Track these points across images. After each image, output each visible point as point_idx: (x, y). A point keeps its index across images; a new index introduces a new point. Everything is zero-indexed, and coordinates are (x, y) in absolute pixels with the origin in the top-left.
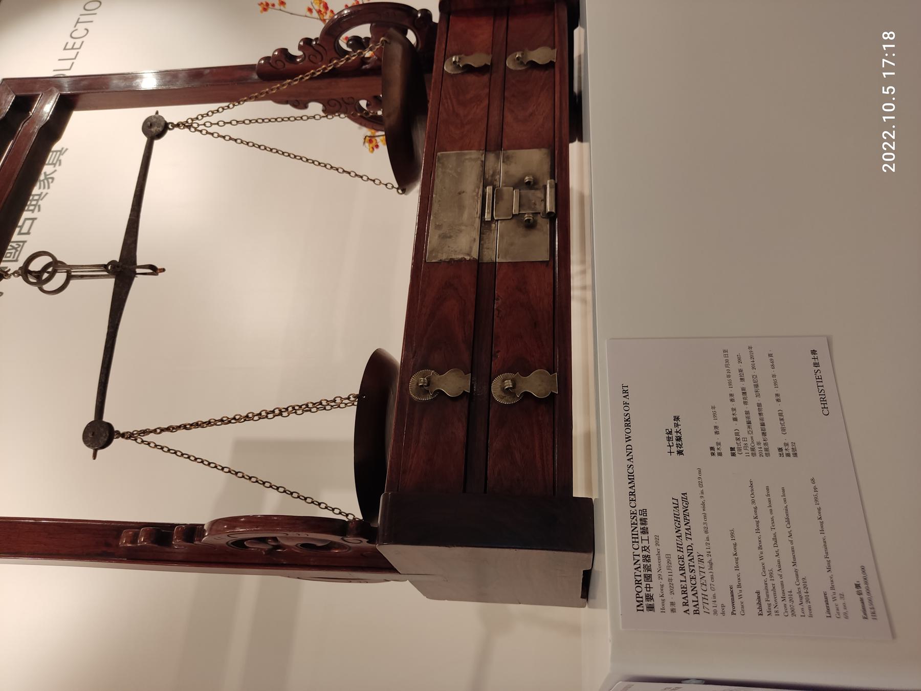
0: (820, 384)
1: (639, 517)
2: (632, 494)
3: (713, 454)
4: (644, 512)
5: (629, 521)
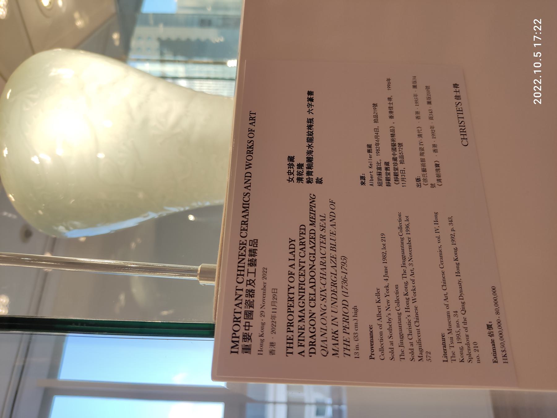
0: (460, 116)
1: (248, 247)
2: (245, 223)
4: (255, 242)
5: (237, 251)
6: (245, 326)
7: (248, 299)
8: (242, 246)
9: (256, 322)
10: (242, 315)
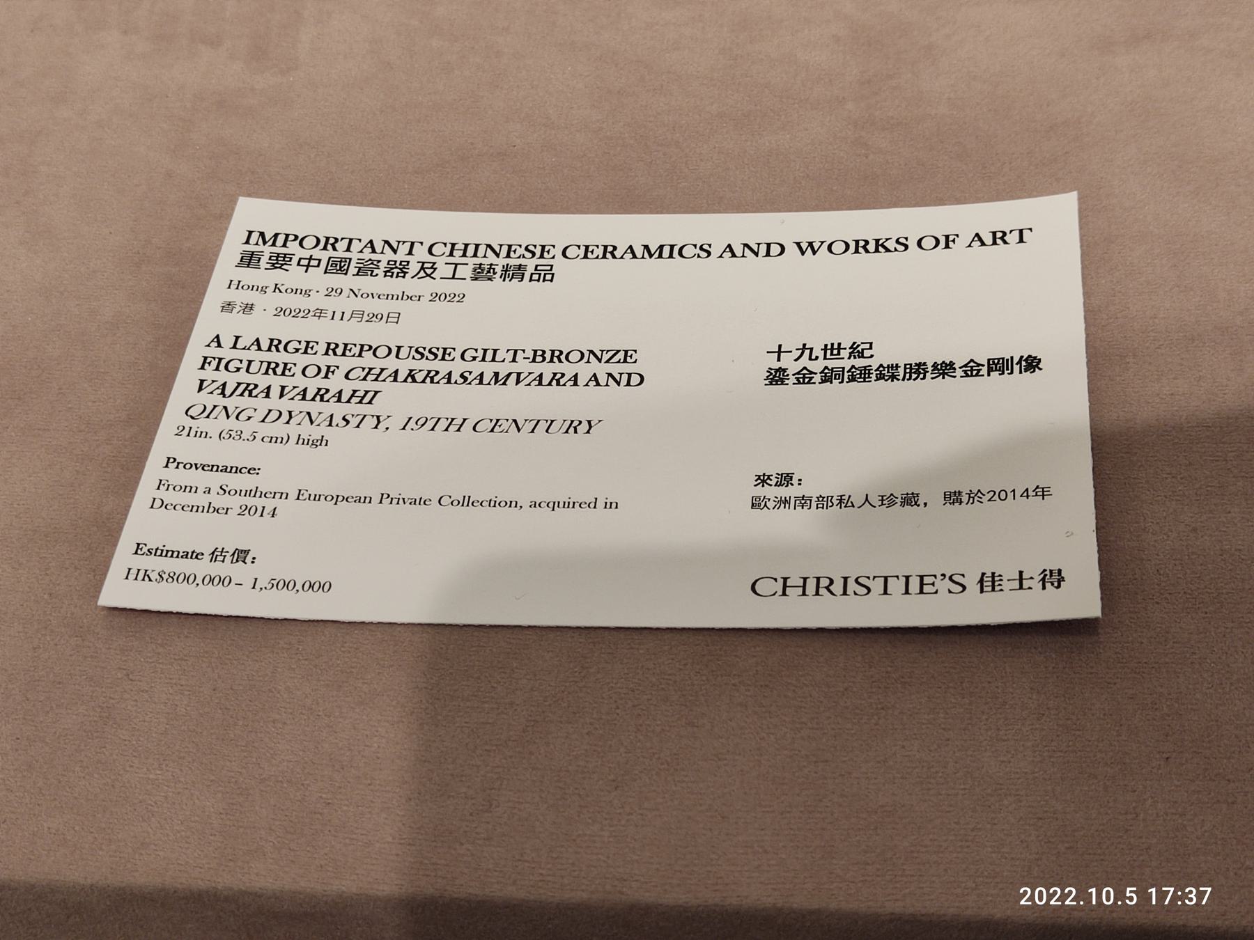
1: (530, 264)
3: (763, 480)
4: (544, 275)
6: (311, 258)
7: (383, 265)
8: (538, 251)
9: (317, 279)
10: (341, 253)
